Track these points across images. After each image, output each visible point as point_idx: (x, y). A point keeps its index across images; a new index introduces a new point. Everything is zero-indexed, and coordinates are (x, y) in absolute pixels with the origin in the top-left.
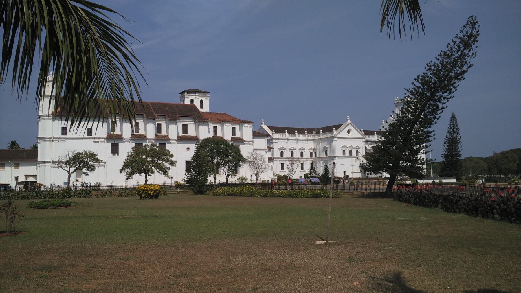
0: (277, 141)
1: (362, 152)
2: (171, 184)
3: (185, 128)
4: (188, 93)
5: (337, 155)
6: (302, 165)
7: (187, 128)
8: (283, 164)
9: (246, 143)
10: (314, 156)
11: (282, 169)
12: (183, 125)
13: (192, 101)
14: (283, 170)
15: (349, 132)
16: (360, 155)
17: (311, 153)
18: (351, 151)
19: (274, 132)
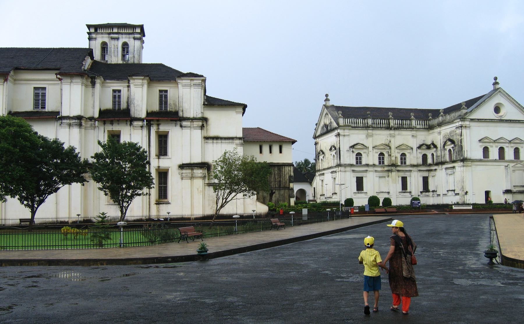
0: (347, 132)
2: (55, 220)
4: (96, 30)
5: (469, 157)
6: (404, 181)
7: (44, 95)
8: (363, 177)
9: (184, 123)
10: (430, 161)
11: (358, 190)
12: (34, 88)
14: (363, 190)
15: (497, 109)
17: (425, 157)
18: (501, 151)
19: (340, 115)
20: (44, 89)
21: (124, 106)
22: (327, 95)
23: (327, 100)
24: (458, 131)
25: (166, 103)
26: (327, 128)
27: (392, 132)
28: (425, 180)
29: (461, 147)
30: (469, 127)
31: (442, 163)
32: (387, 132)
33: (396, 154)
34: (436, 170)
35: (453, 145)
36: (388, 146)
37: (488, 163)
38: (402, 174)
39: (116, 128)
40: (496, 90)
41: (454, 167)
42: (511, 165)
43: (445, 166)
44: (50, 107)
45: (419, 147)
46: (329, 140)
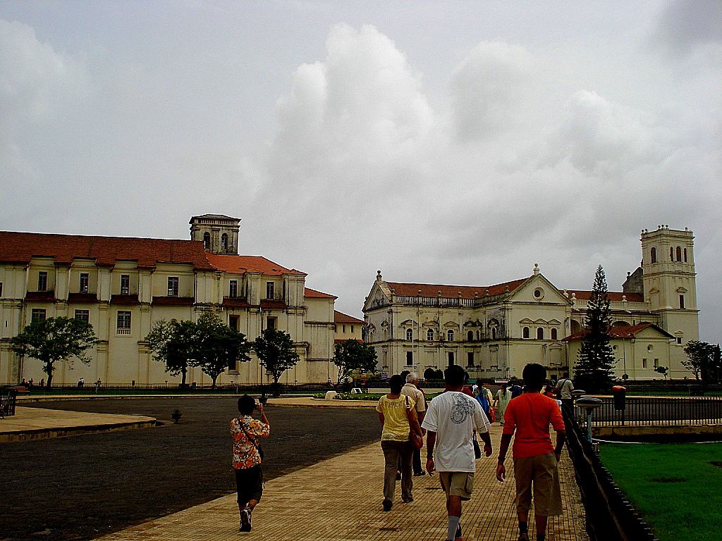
1: (564, 332)
3: (173, 283)
4: (200, 222)
10: (475, 338)
13: (207, 237)
15: (537, 293)
16: (560, 337)
17: (470, 334)
18: (540, 331)
20: (177, 278)
21: (238, 294)
22: (379, 272)
23: (379, 277)
24: (502, 313)
25: (272, 293)
26: (378, 303)
27: (440, 310)
28: (471, 356)
29: (503, 327)
30: (511, 309)
31: (488, 340)
32: (436, 310)
33: (444, 331)
34: (480, 346)
35: (496, 325)
36: (437, 323)
37: (527, 342)
38: (449, 350)
39: (236, 313)
40: (537, 277)
41: (497, 345)
42: (549, 344)
43: (489, 344)
44: (181, 294)
45: (465, 325)
46: (382, 315)
